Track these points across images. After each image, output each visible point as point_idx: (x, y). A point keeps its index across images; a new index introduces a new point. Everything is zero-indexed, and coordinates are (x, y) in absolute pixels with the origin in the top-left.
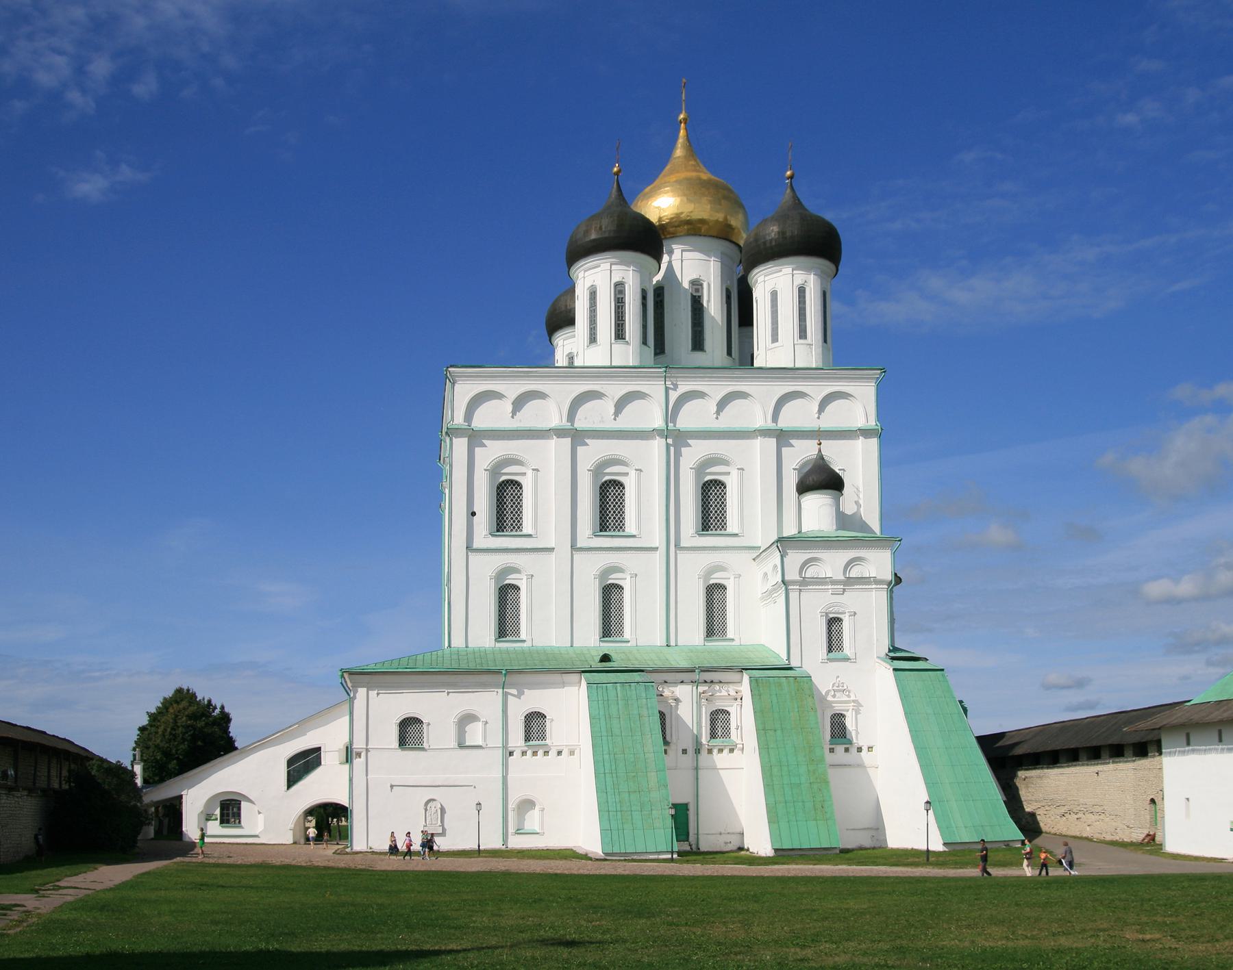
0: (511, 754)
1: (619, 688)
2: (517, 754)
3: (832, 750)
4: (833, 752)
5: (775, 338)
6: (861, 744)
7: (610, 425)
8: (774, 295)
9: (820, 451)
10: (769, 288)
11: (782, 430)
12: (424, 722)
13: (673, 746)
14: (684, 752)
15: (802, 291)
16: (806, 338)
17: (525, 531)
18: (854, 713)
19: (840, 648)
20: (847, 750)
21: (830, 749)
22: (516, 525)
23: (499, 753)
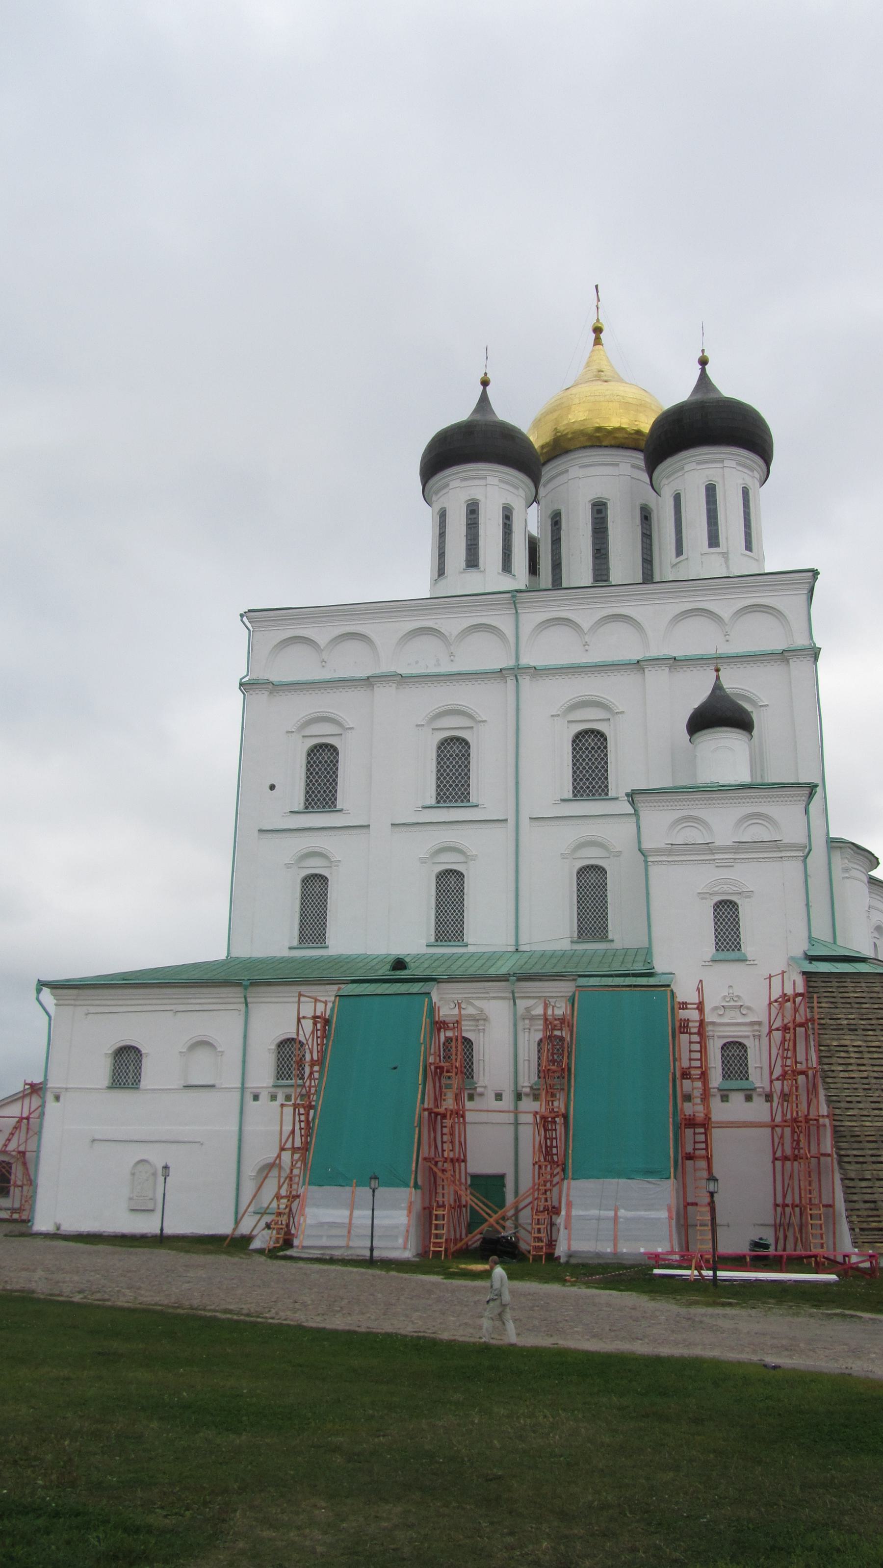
0: (256, 1098)
2: (264, 1096)
3: (725, 1098)
4: (727, 1101)
5: (679, 551)
8: (677, 498)
9: (718, 678)
11: (675, 658)
12: (143, 1051)
15: (711, 491)
17: (338, 807)
18: (757, 1040)
19: (738, 946)
20: (749, 1098)
21: (722, 1096)
22: (330, 799)
23: (237, 1095)
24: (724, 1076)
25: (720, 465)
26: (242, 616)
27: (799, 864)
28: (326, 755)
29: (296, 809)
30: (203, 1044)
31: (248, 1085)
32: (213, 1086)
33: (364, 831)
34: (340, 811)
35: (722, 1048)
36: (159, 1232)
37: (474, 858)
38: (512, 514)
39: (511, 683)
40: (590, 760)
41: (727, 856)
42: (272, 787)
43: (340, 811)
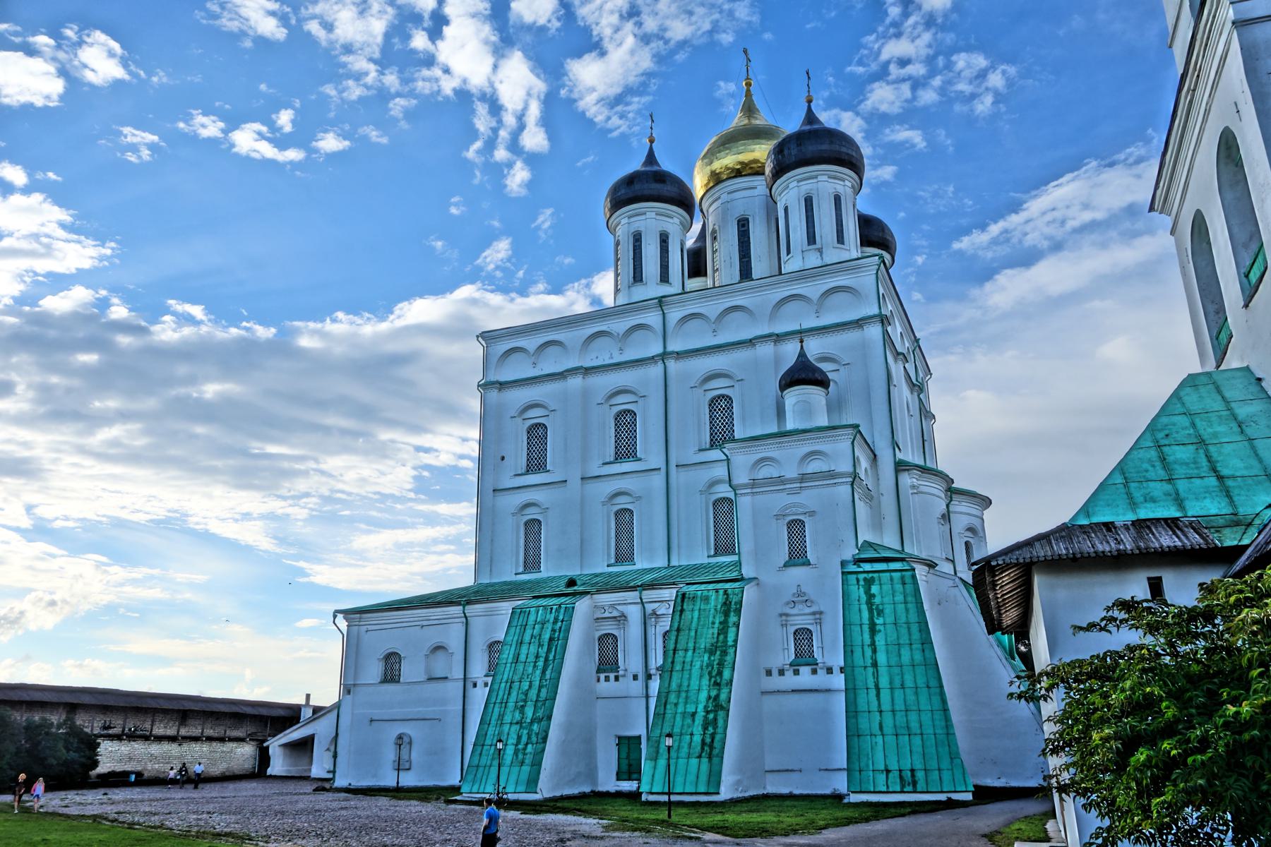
0: (475, 685)
1: (540, 612)
3: (796, 672)
4: (798, 674)
5: (788, 252)
6: (829, 664)
7: (618, 358)
8: (786, 209)
9: (802, 347)
10: (783, 202)
13: (621, 673)
14: (635, 677)
15: (809, 202)
16: (814, 243)
18: (819, 627)
20: (814, 672)
24: (796, 655)
25: (815, 180)
26: (478, 337)
27: (849, 488)
28: (541, 432)
29: (520, 473)
30: (439, 648)
31: (468, 676)
32: (446, 678)
33: (564, 484)
34: (549, 471)
35: (795, 633)
36: (395, 785)
37: (639, 498)
38: (668, 238)
39: (660, 364)
40: (722, 418)
41: (795, 485)
42: (503, 458)
43: (549, 471)
